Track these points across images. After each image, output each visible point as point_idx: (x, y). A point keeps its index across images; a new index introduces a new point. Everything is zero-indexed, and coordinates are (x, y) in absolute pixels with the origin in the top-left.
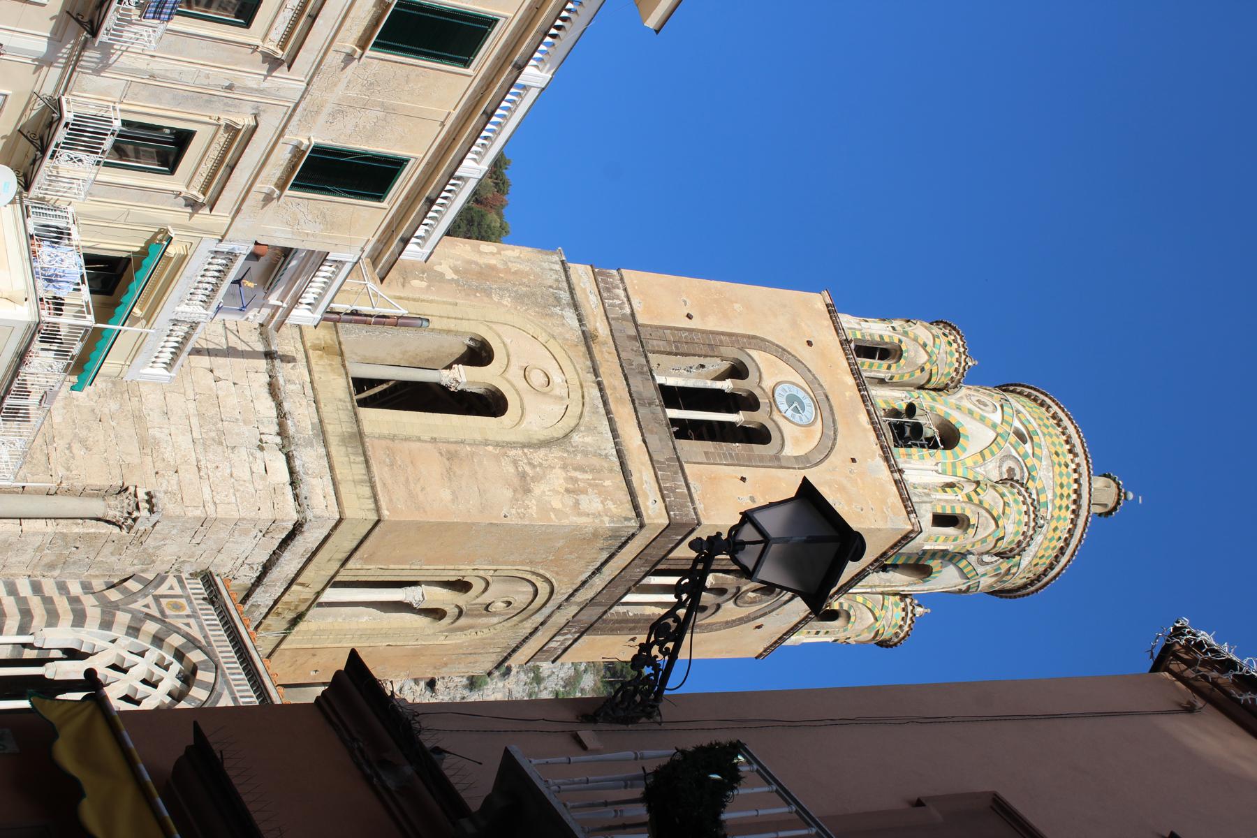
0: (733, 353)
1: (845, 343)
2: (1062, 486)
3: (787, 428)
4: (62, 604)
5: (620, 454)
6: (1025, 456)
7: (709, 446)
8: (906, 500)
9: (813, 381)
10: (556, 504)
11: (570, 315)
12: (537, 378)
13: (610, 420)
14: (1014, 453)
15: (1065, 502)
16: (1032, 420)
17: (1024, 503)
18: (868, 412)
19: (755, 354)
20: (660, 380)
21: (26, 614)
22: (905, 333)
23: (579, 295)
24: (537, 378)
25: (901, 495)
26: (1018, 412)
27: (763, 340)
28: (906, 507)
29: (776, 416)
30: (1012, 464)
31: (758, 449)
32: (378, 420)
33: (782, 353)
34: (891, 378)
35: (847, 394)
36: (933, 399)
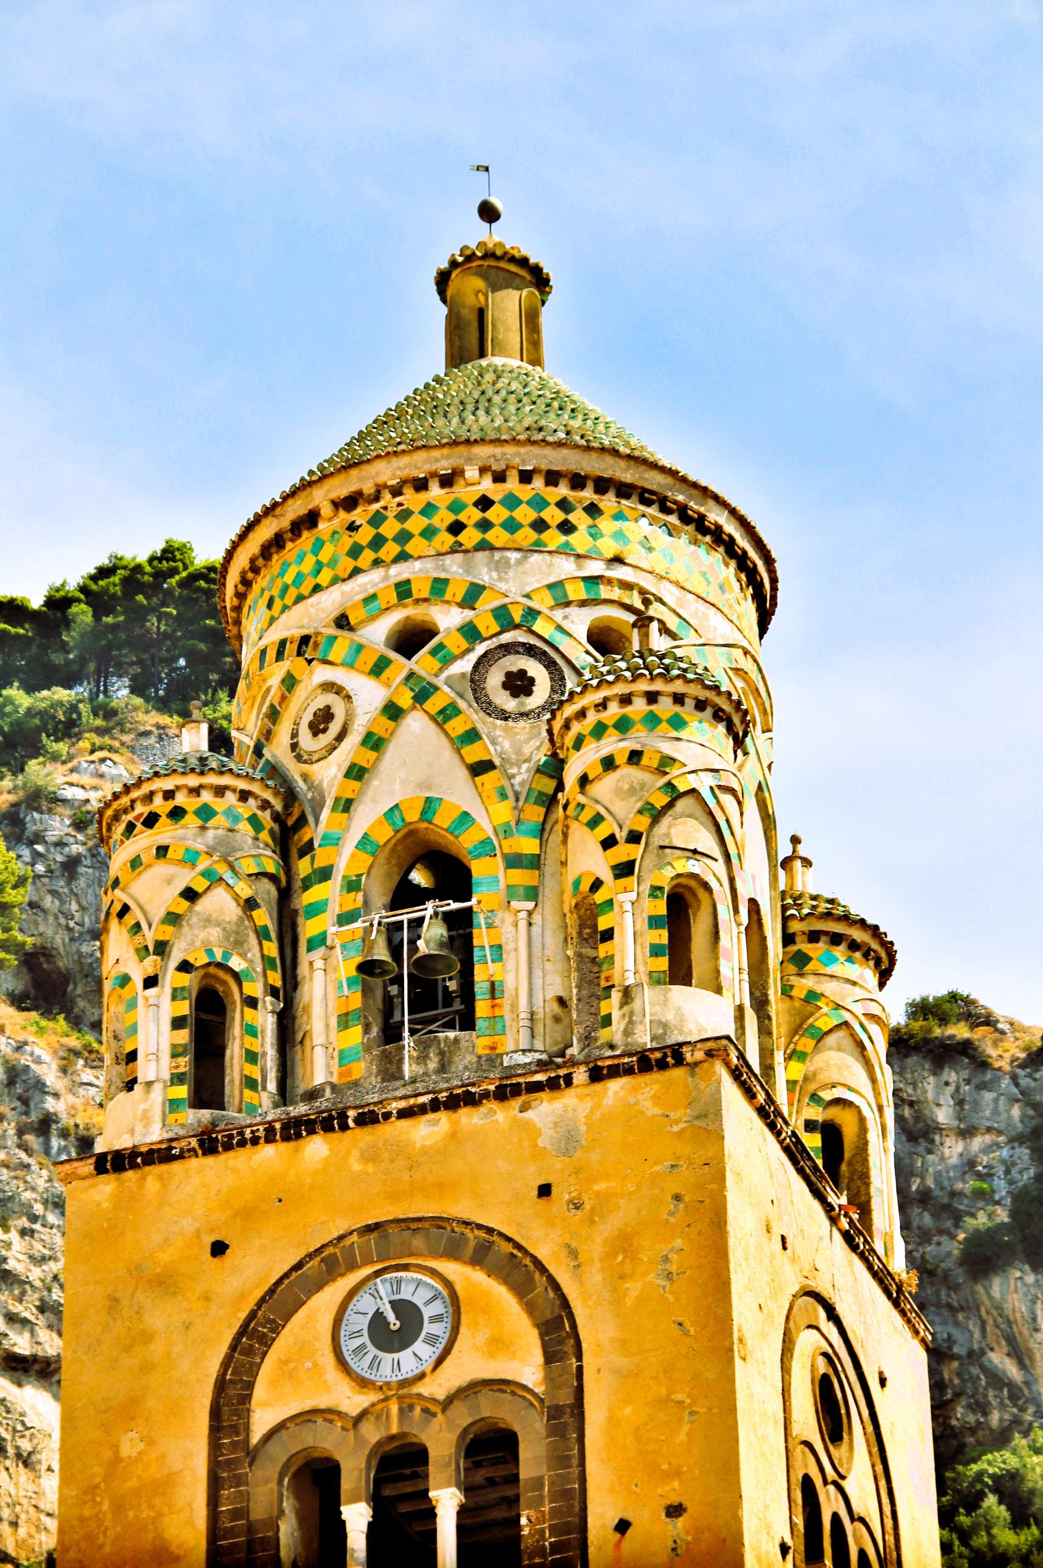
1: (210, 1143)
2: (540, 526)
3: (467, 1365)
6: (471, 633)
8: (645, 1063)
9: (325, 1263)
14: (465, 665)
15: (579, 517)
16: (361, 579)
17: (626, 700)
18: (403, 1114)
22: (162, 948)
25: (629, 1071)
26: (342, 622)
27: (221, 1385)
28: (662, 1065)
29: (437, 1387)
30: (494, 679)
31: (532, 1459)
34: (274, 992)
35: (357, 1167)
36: (325, 874)
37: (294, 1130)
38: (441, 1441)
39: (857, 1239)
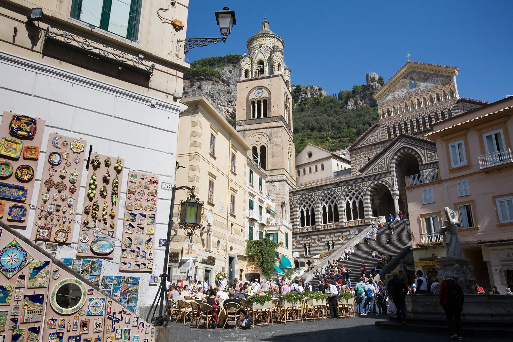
0: (250, 103)
1: (246, 81)
4: (294, 213)
5: (271, 128)
7: (268, 111)
10: (280, 140)
11: (246, 132)
12: (258, 140)
13: (266, 128)
19: (250, 99)
20: (256, 118)
21: (296, 218)
23: (241, 130)
24: (258, 140)
29: (261, 97)
31: (268, 102)
32: (268, 166)
33: (249, 93)
37: (252, 80)
38: (262, 100)
39: (288, 89)
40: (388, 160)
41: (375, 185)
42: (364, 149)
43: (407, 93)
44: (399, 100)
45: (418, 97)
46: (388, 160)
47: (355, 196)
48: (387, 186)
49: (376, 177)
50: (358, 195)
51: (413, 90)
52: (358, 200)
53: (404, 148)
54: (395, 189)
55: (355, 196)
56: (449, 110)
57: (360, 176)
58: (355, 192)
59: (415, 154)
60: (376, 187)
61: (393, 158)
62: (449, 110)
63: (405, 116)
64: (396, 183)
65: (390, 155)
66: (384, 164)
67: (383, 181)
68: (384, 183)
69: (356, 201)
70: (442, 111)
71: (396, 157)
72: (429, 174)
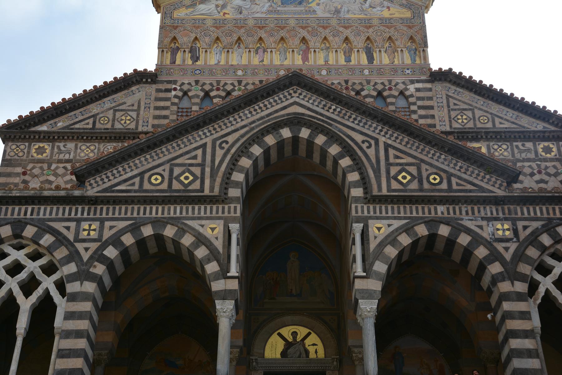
40: (219, 153)
41: (141, 243)
42: (71, 145)
43: (269, 12)
44: (239, 24)
45: (304, 33)
46: (219, 153)
47: (23, 275)
48: (201, 253)
49: (156, 211)
50: (40, 276)
51: (291, 8)
52: (34, 298)
53: (295, 122)
54: (234, 271)
55: (23, 275)
56: (402, 93)
57: (77, 193)
58: (25, 261)
59: (341, 156)
60: (135, 254)
61: (244, 151)
62: (402, 93)
63: (254, 74)
64: (235, 250)
65: (231, 139)
66: (202, 165)
67: (182, 231)
68: (187, 240)
69: (20, 298)
70: (380, 94)
71: (257, 150)
72: (391, 239)
